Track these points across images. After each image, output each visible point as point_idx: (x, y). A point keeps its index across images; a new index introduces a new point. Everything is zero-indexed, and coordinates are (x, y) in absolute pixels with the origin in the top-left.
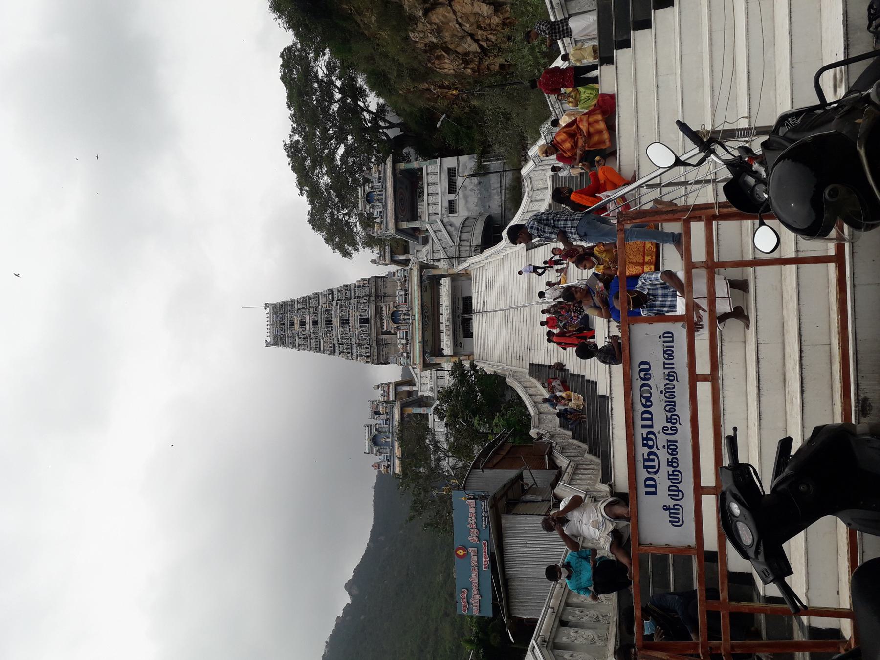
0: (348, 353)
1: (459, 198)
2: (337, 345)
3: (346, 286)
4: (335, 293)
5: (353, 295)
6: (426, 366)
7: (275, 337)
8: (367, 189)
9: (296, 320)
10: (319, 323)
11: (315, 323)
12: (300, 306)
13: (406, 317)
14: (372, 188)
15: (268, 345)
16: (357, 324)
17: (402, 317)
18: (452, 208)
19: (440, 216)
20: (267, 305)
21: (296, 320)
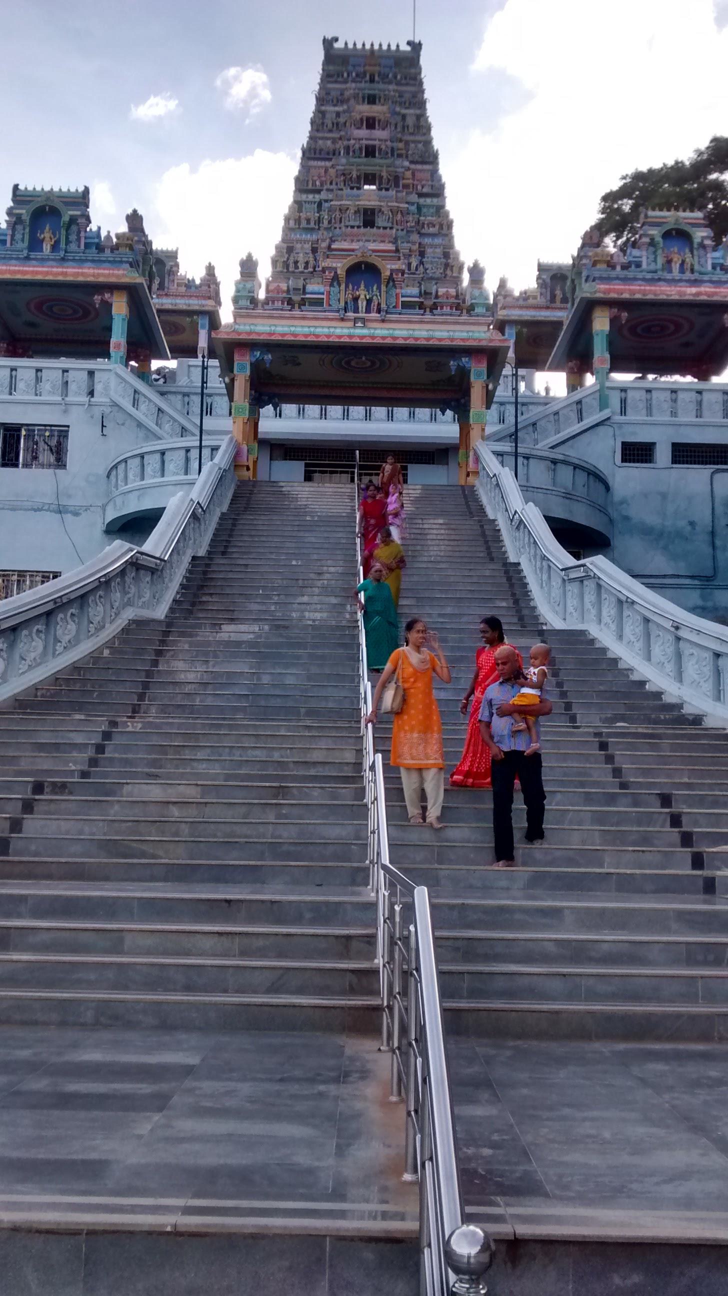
1: (662, 472)
2: (317, 197)
4: (435, 200)
5: (427, 241)
8: (701, 234)
9: (377, 110)
10: (371, 160)
11: (370, 152)
12: (410, 121)
13: (362, 304)
14: (702, 246)
15: (328, 44)
17: (362, 293)
18: (637, 453)
19: (618, 418)
20: (416, 47)
21: (377, 110)
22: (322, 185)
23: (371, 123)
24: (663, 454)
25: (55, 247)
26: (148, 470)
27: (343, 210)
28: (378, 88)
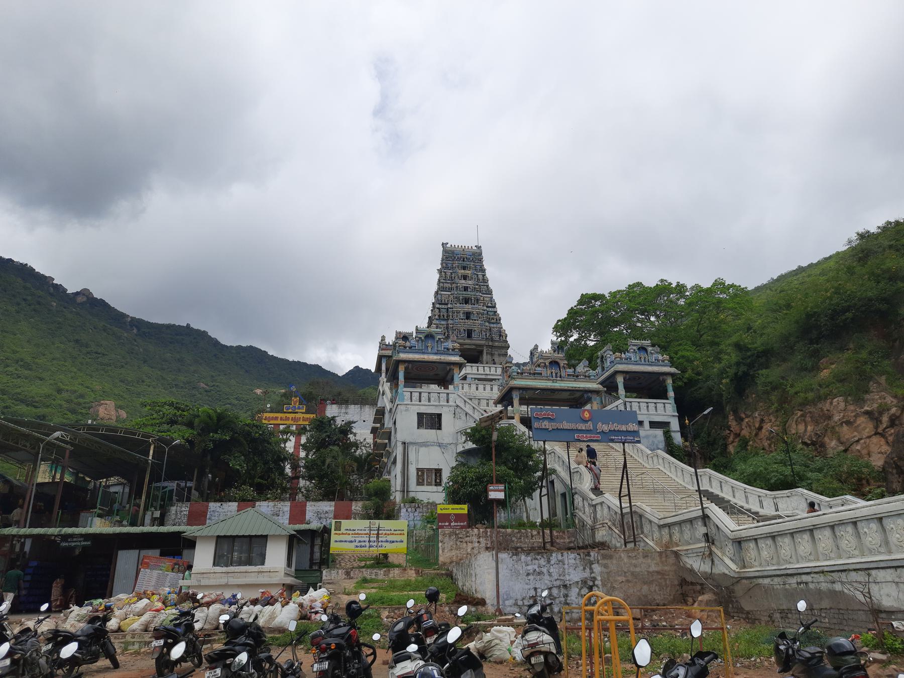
5: (492, 325)
7: (453, 252)
8: (650, 349)
9: (468, 272)
11: (466, 289)
12: (480, 277)
16: (467, 327)
21: (468, 272)
27: (458, 312)
28: (466, 263)
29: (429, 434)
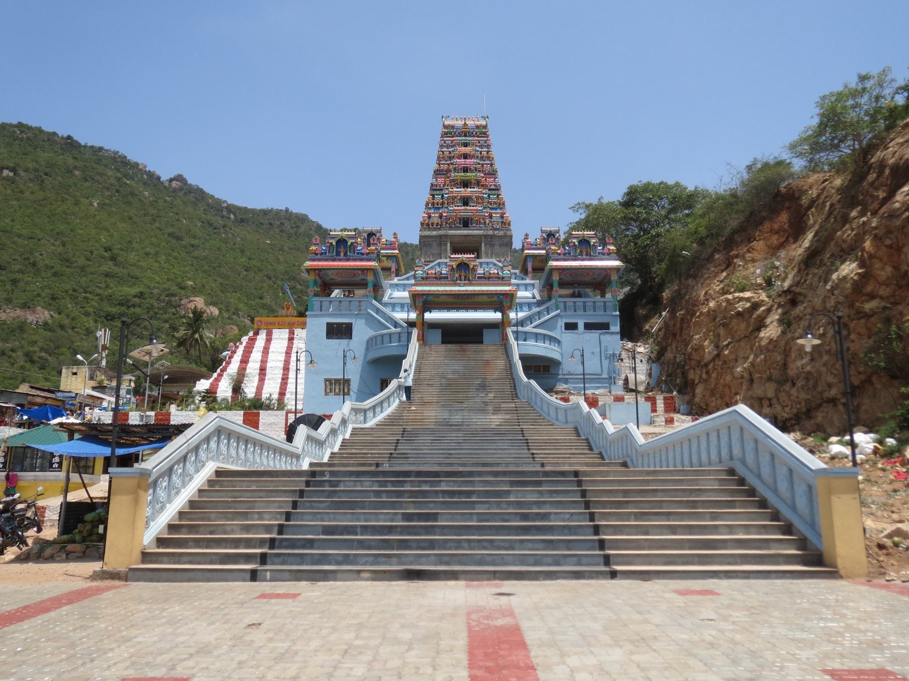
0: (433, 204)
3: (503, 204)
6: (415, 296)
11: (466, 170)
13: (463, 278)
18: (571, 327)
22: (444, 186)
23: (466, 156)
24: (581, 326)
25: (345, 254)
26: (385, 341)
29: (339, 344)
